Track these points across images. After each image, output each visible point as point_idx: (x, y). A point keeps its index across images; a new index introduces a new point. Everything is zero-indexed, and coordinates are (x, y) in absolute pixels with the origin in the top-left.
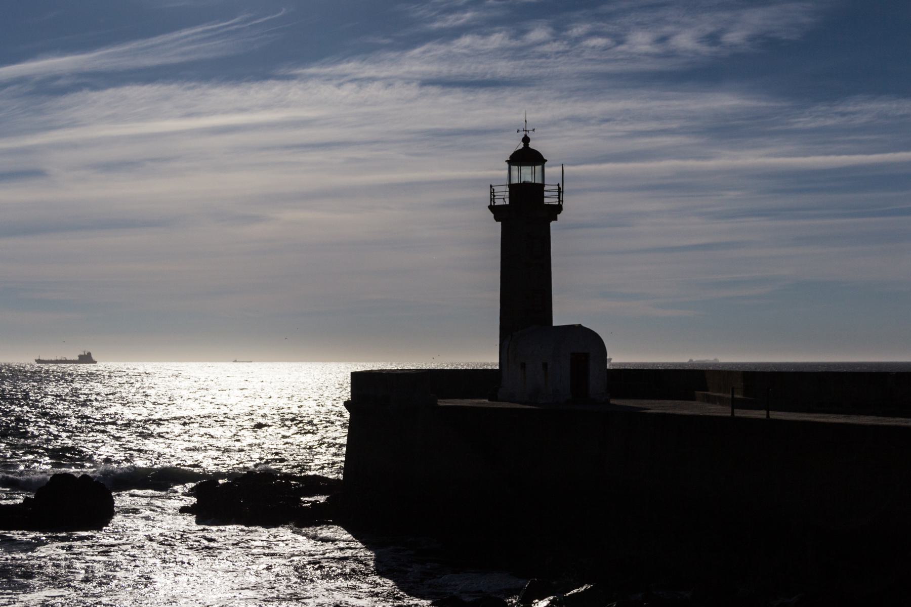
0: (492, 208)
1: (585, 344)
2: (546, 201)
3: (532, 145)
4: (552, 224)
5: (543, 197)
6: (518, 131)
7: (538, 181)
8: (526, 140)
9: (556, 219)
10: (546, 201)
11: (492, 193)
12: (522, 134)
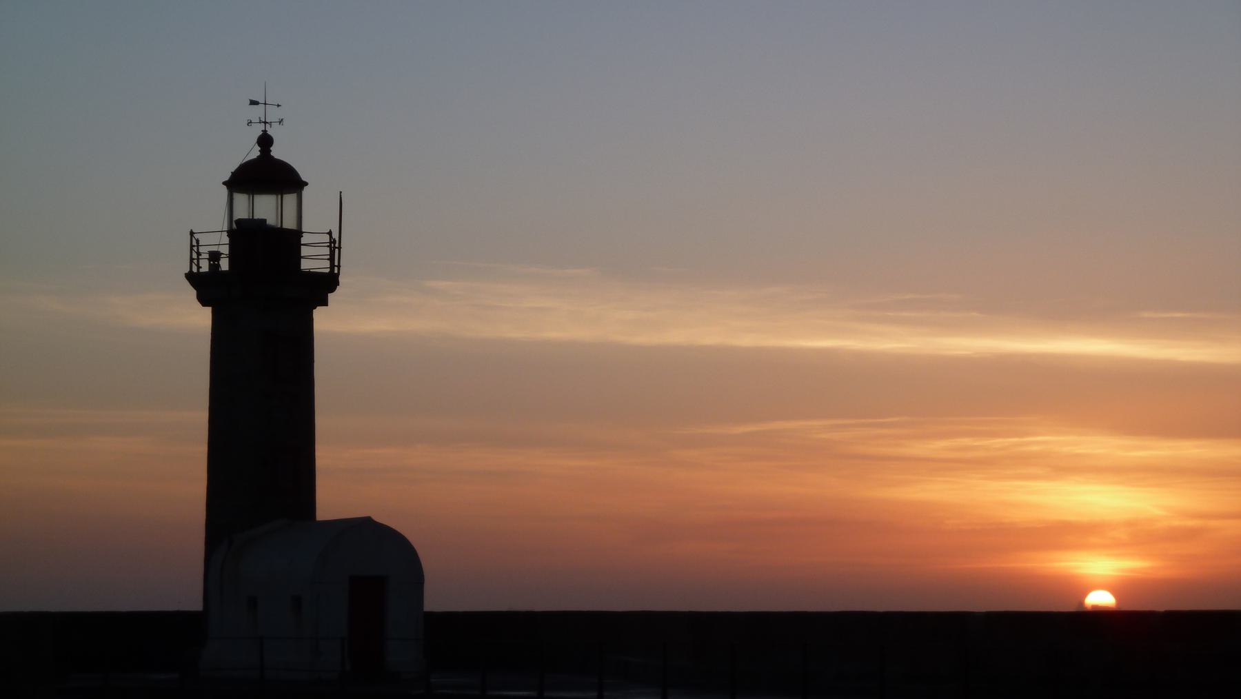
0: (193, 278)
2: (305, 265)
3: (277, 152)
5: (298, 257)
6: (250, 123)
7: (289, 223)
8: (265, 141)
9: (325, 303)
10: (305, 265)
11: (194, 246)
12: (257, 130)
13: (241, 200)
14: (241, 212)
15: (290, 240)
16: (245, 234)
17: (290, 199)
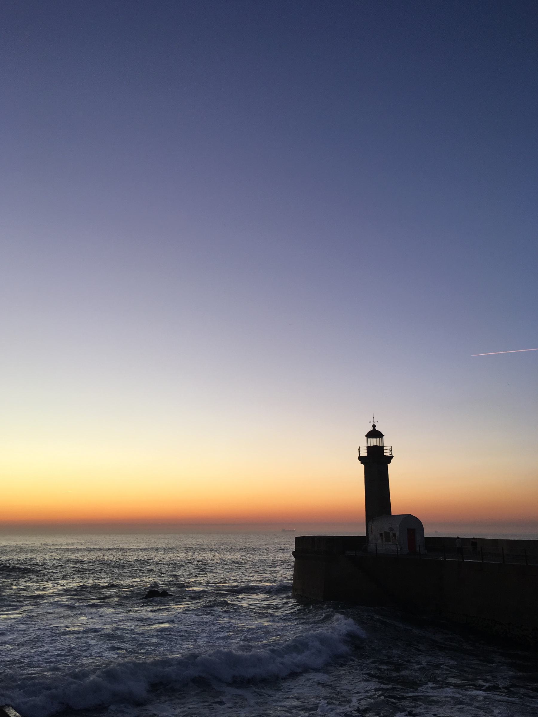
1: (411, 524)
2: (385, 454)
3: (377, 428)
8: (374, 426)
10: (385, 454)
12: (372, 424)
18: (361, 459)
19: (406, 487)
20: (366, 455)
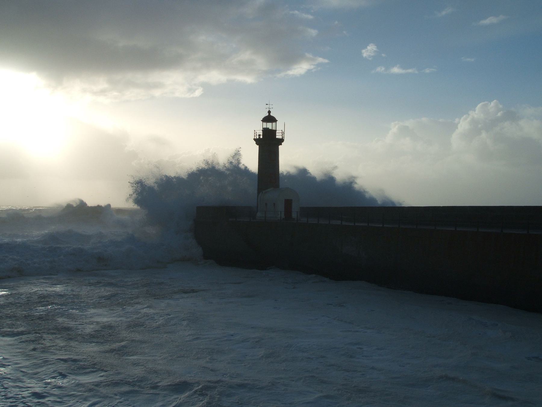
2: (277, 137)
3: (271, 114)
4: (280, 146)
5: (275, 135)
7: (274, 129)
8: (269, 112)
10: (277, 137)
13: (265, 124)
14: (265, 127)
15: (274, 132)
16: (265, 130)
17: (274, 124)
18: (258, 141)
19: (289, 159)
20: (261, 137)
